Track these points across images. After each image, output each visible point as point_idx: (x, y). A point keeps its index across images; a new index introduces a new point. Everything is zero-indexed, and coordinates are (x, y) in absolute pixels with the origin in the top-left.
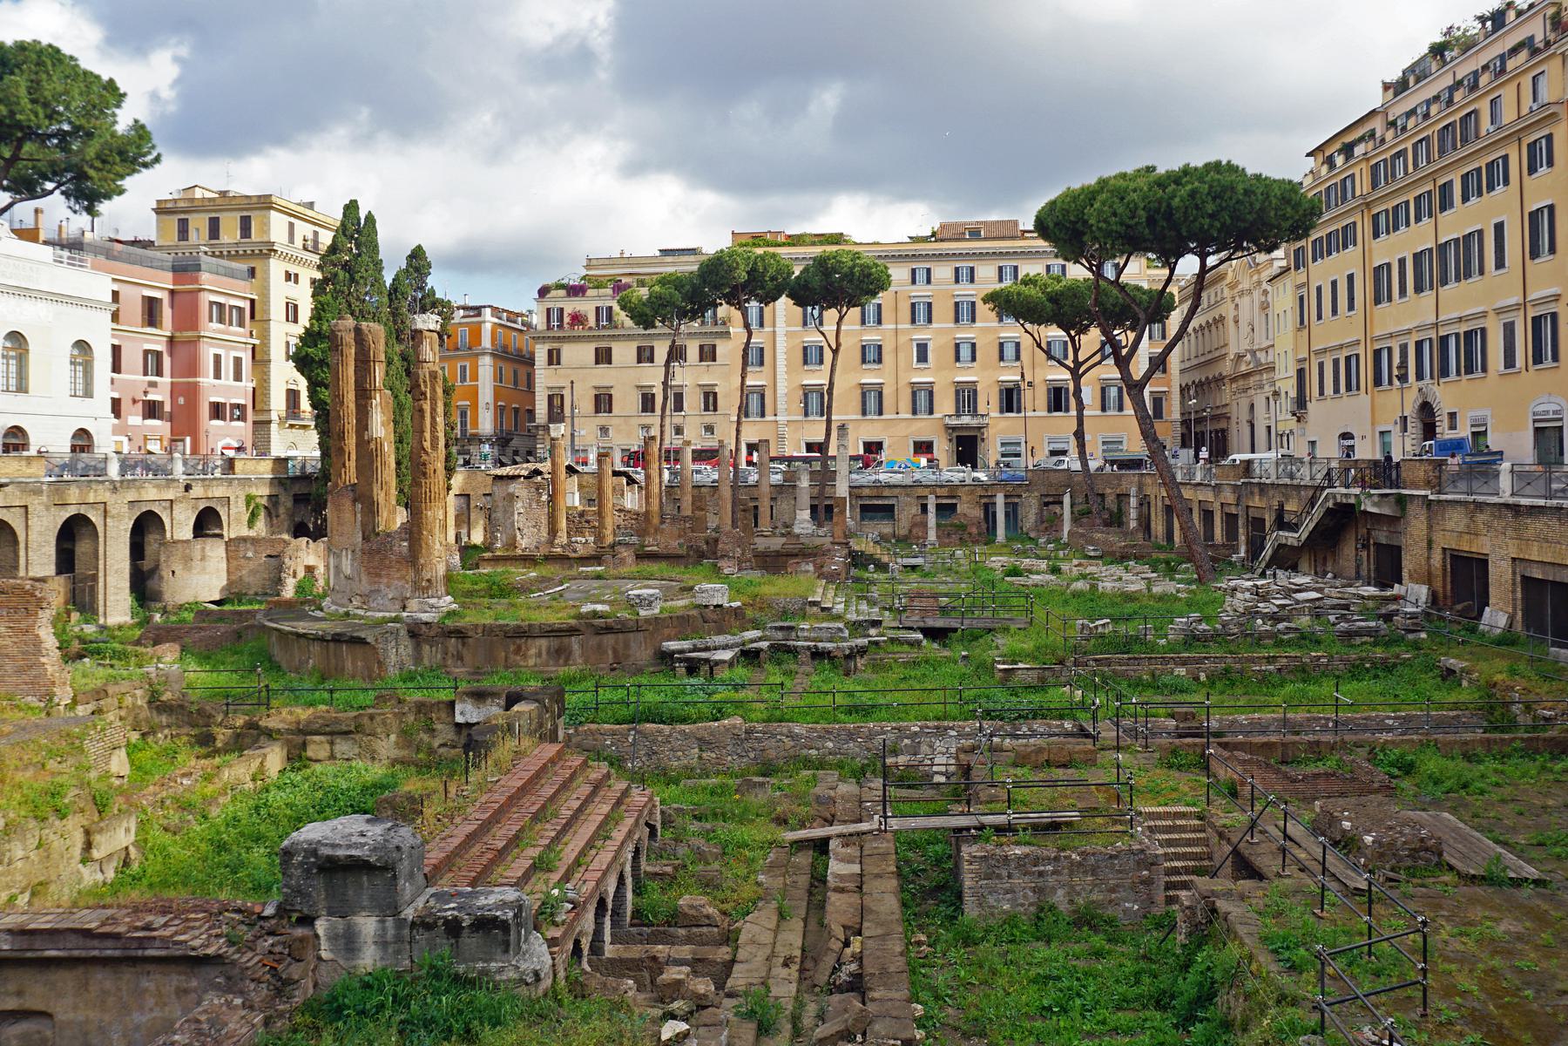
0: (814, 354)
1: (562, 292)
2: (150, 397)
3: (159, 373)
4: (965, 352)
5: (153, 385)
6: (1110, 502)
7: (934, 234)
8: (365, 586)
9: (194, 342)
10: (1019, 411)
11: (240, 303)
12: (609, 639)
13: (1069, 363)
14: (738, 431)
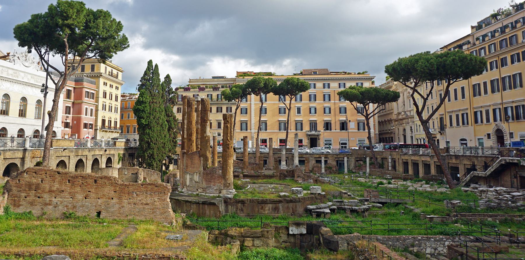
0: (282, 111)
1: (182, 90)
2: (67, 121)
3: (69, 114)
4: (313, 111)
5: (67, 117)
6: (379, 160)
7: (301, 73)
8: (204, 185)
9: (80, 104)
10: (346, 130)
11: (93, 92)
12: (291, 205)
13: (365, 114)
14: (258, 135)
